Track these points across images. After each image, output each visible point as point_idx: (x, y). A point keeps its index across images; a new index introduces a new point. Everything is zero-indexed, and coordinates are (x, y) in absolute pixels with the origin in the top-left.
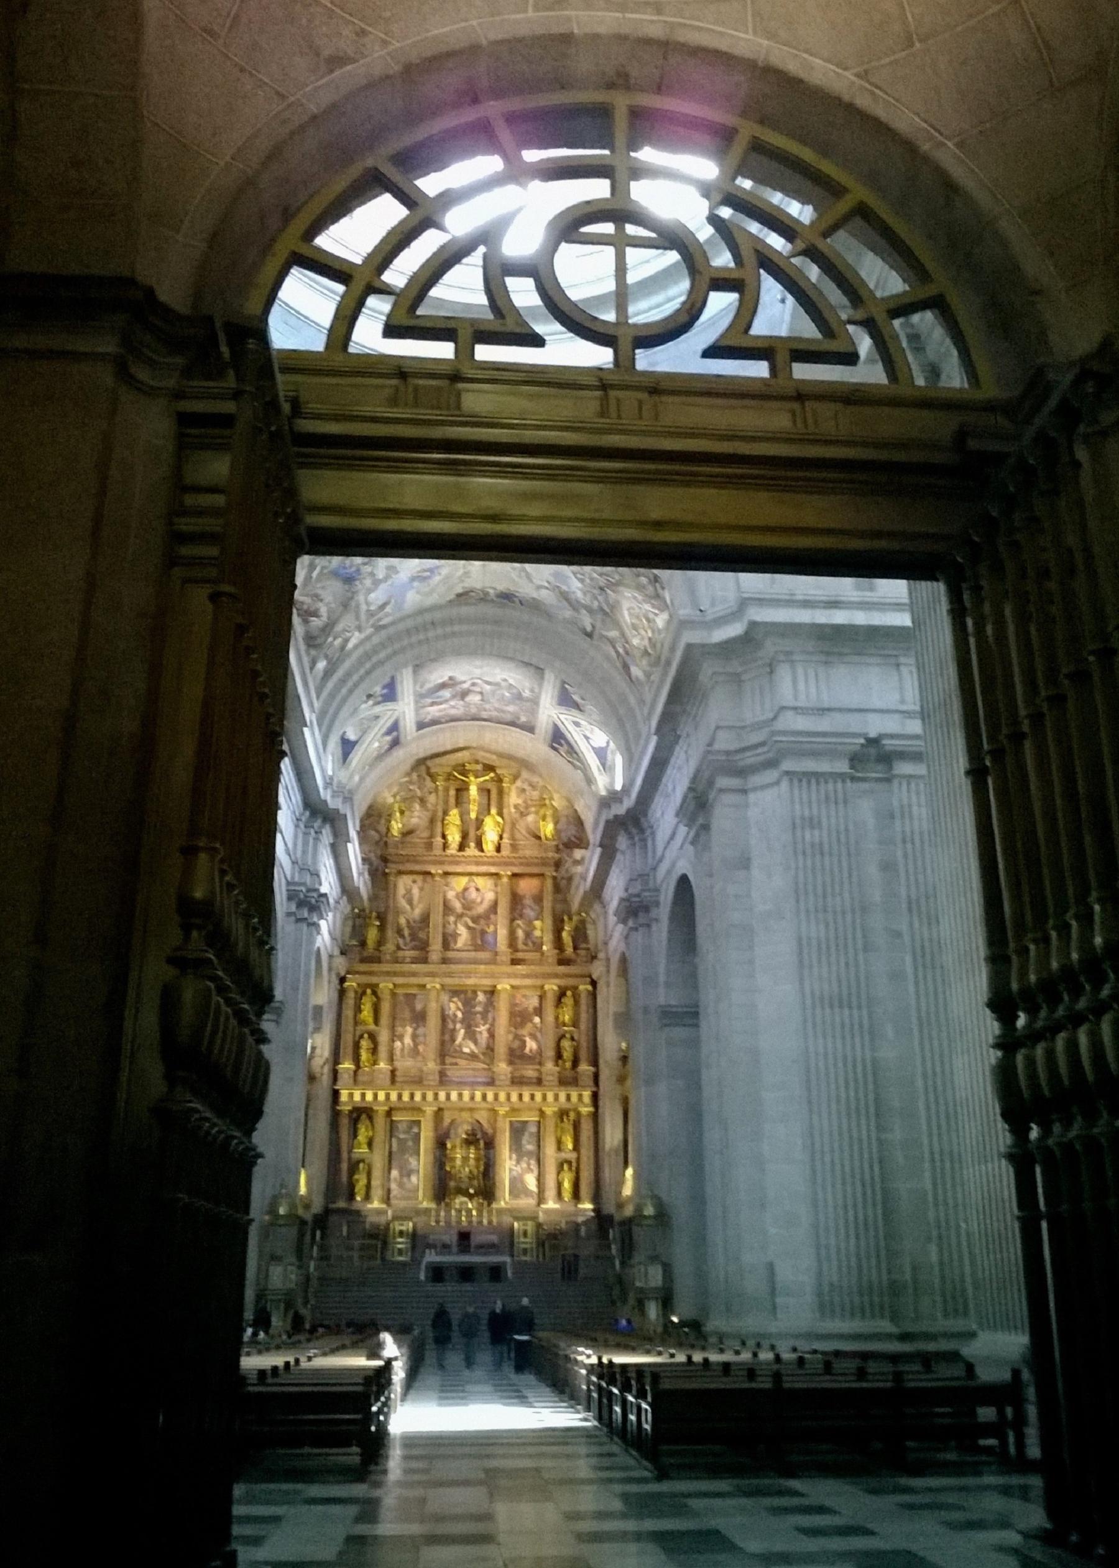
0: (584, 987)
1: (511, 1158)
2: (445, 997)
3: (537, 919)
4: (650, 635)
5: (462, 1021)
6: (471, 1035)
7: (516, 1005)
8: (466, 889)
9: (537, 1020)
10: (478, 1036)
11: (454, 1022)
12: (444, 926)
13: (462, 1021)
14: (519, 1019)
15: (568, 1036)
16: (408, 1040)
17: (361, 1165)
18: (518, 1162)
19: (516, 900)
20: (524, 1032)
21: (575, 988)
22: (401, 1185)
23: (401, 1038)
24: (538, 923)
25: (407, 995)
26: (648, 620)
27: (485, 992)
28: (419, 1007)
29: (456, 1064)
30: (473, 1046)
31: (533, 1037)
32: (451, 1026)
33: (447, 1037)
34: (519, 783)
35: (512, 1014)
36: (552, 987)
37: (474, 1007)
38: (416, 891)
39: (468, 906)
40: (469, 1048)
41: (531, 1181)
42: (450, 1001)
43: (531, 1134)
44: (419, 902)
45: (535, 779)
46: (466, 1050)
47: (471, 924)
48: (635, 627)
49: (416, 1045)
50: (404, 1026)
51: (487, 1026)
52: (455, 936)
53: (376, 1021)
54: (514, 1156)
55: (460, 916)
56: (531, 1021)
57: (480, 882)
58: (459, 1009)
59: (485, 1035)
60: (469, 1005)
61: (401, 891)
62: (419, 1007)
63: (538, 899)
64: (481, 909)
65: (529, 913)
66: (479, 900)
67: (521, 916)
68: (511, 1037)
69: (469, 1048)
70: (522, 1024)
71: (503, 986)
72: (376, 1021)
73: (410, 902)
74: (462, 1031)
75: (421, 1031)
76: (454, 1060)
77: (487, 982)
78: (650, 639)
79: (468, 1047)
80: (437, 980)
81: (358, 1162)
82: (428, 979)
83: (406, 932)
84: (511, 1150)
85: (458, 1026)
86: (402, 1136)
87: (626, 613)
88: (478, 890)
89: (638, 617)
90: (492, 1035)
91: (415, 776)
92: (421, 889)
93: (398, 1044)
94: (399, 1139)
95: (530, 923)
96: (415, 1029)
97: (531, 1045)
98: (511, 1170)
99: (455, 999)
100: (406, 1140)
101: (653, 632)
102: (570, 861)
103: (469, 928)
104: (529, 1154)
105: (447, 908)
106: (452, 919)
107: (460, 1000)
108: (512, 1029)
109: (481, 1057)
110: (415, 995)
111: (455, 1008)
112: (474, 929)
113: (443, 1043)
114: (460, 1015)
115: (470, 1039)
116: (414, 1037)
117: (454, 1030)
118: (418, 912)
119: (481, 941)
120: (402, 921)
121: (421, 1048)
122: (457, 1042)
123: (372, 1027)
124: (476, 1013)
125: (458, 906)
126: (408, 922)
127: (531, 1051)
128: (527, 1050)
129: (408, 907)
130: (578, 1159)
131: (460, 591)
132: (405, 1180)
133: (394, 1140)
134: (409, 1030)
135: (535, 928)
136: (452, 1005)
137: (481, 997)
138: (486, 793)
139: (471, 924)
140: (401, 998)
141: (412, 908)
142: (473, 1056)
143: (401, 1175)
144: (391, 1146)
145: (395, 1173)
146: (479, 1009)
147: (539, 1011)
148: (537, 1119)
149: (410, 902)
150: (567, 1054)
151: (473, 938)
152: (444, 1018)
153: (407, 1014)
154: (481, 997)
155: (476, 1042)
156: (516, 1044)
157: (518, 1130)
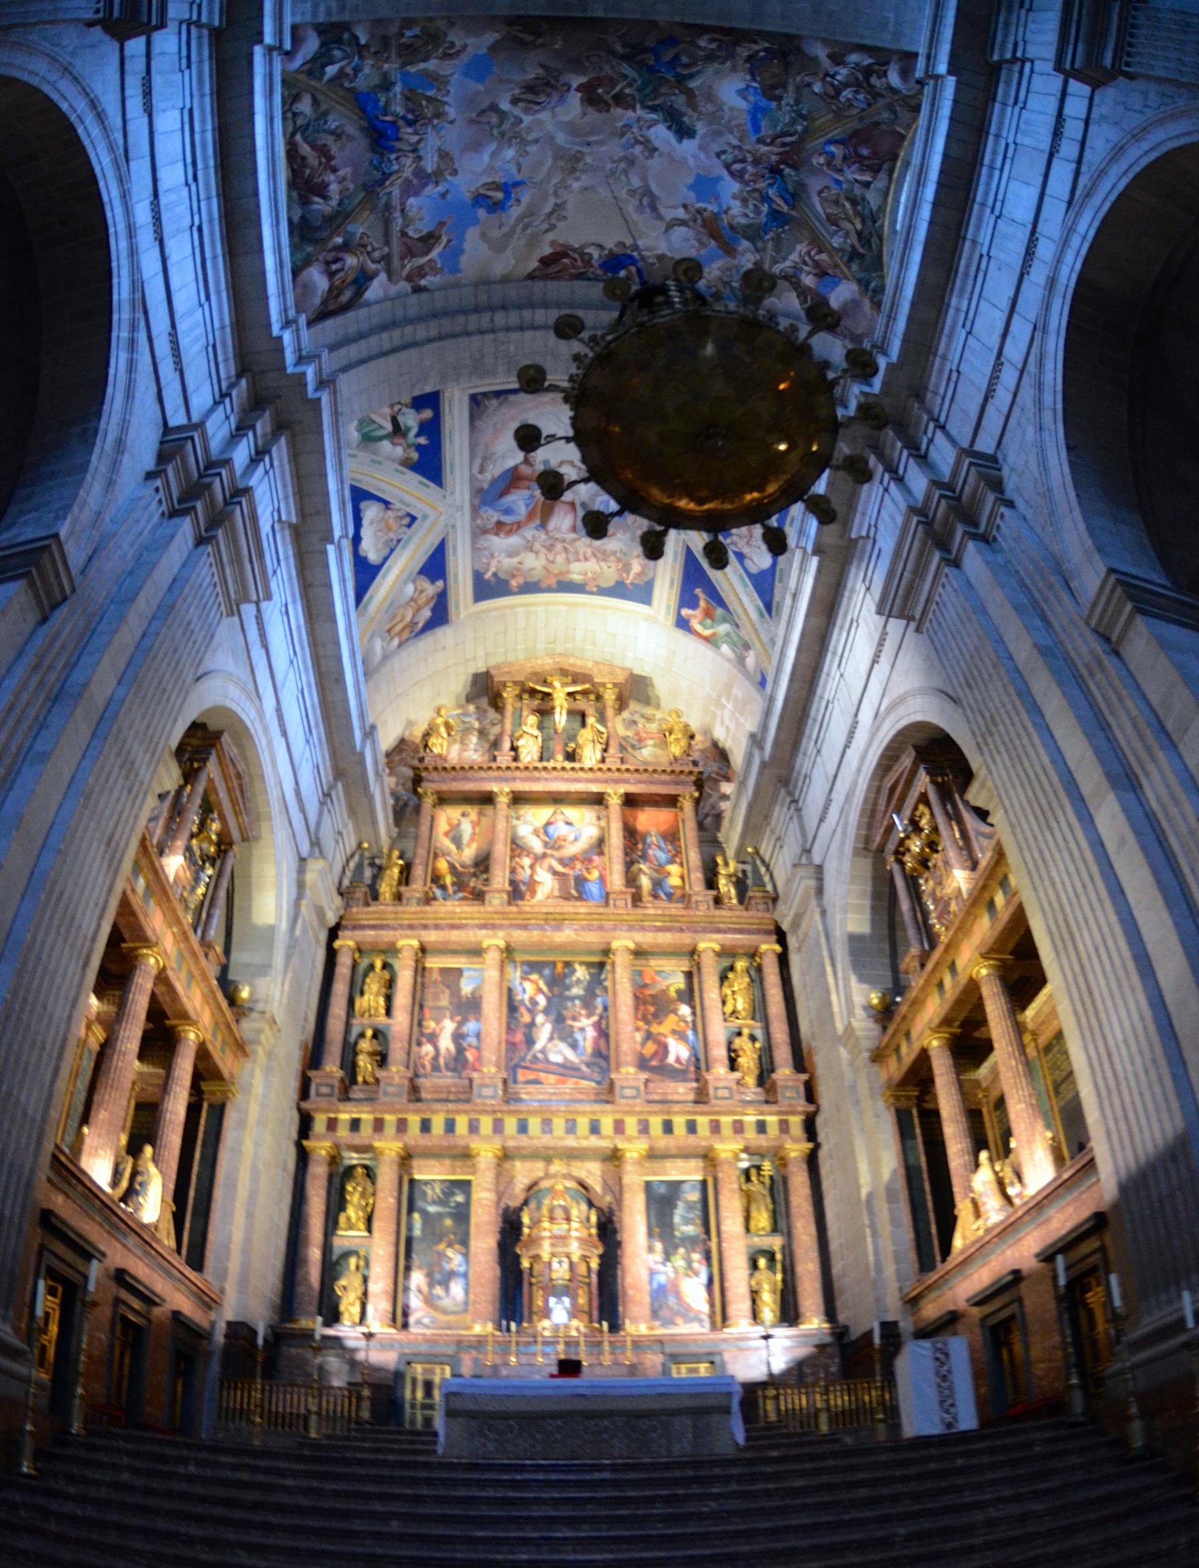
0: (769, 947)
1: (651, 1249)
2: (515, 975)
3: (672, 862)
4: (859, 226)
5: (546, 1011)
6: (563, 1031)
7: (646, 986)
8: (548, 824)
9: (685, 1010)
10: (578, 1036)
11: (532, 1012)
12: (513, 871)
13: (546, 1011)
14: (652, 1009)
15: (746, 1031)
16: (446, 1043)
17: (353, 1261)
18: (668, 1256)
19: (632, 835)
20: (663, 1028)
21: (753, 954)
22: (430, 1301)
23: (433, 1038)
24: (674, 869)
25: (444, 971)
26: (854, 203)
27: (589, 965)
28: (466, 988)
29: (537, 1082)
30: (571, 1055)
31: (680, 1036)
32: (526, 1018)
33: (519, 1037)
34: (626, 714)
35: (640, 1000)
36: (708, 944)
37: (568, 988)
38: (466, 828)
39: (553, 844)
40: (560, 1053)
41: (694, 1292)
42: (524, 978)
43: (690, 1206)
44: (472, 839)
45: (649, 711)
46: (555, 1058)
47: (559, 868)
48: (833, 220)
49: (460, 1050)
50: (438, 1021)
51: (595, 1019)
52: (532, 884)
53: (388, 1012)
54: (659, 1246)
55: (538, 859)
56: (675, 1012)
57: (572, 812)
58: (540, 991)
59: (591, 1033)
60: (557, 983)
61: (442, 825)
62: (466, 988)
63: (671, 837)
64: (571, 850)
65: (658, 854)
66: (571, 838)
67: (644, 857)
68: (639, 1037)
69: (560, 1053)
70: (659, 1016)
71: (622, 942)
72: (388, 1012)
73: (457, 841)
74: (548, 1028)
75: (471, 1027)
76: (532, 1076)
77: (593, 938)
78: (859, 234)
79: (560, 1052)
80: (501, 934)
81: (347, 1254)
82: (484, 932)
83: (448, 880)
84: (650, 1234)
85: (540, 1019)
86: (432, 1209)
87: (816, 200)
88: (568, 823)
89: (837, 202)
90: (603, 1033)
91: (471, 708)
92: (475, 825)
93: (428, 1049)
94: (424, 1214)
95: (660, 868)
96: (460, 1024)
97: (678, 1051)
98: (652, 1273)
99: (534, 977)
100: (440, 1216)
101: (863, 222)
102: (715, 796)
103: (555, 873)
104: (690, 1242)
105: (517, 847)
106: (526, 862)
107: (542, 976)
108: (641, 1024)
109: (584, 1068)
110: (459, 972)
111: (531, 989)
112: (564, 874)
113: (512, 1046)
114: (542, 1001)
115: (562, 1039)
116: (458, 1037)
117: (532, 1024)
118: (469, 853)
119: (573, 888)
120: (442, 865)
121: (470, 1055)
122: (538, 1046)
123: (382, 1019)
124: (573, 999)
125: (537, 846)
126: (452, 867)
127: (678, 1060)
128: (671, 1059)
129: (453, 847)
130: (788, 1250)
131: (548, 251)
132: (439, 1291)
133: (416, 1216)
134: (449, 1026)
135: (669, 874)
136: (528, 985)
137: (581, 973)
138: (579, 718)
139: (559, 868)
140: (436, 976)
141: (459, 846)
142: (567, 1070)
143: (431, 1285)
144: (410, 1228)
145: (417, 1278)
146: (576, 991)
147: (689, 995)
148: (700, 1178)
149: (457, 841)
150: (748, 1060)
151: (564, 887)
152: (512, 1007)
153: (444, 1001)
154: (581, 973)
155: (574, 1046)
156: (650, 1048)
157: (662, 1202)
